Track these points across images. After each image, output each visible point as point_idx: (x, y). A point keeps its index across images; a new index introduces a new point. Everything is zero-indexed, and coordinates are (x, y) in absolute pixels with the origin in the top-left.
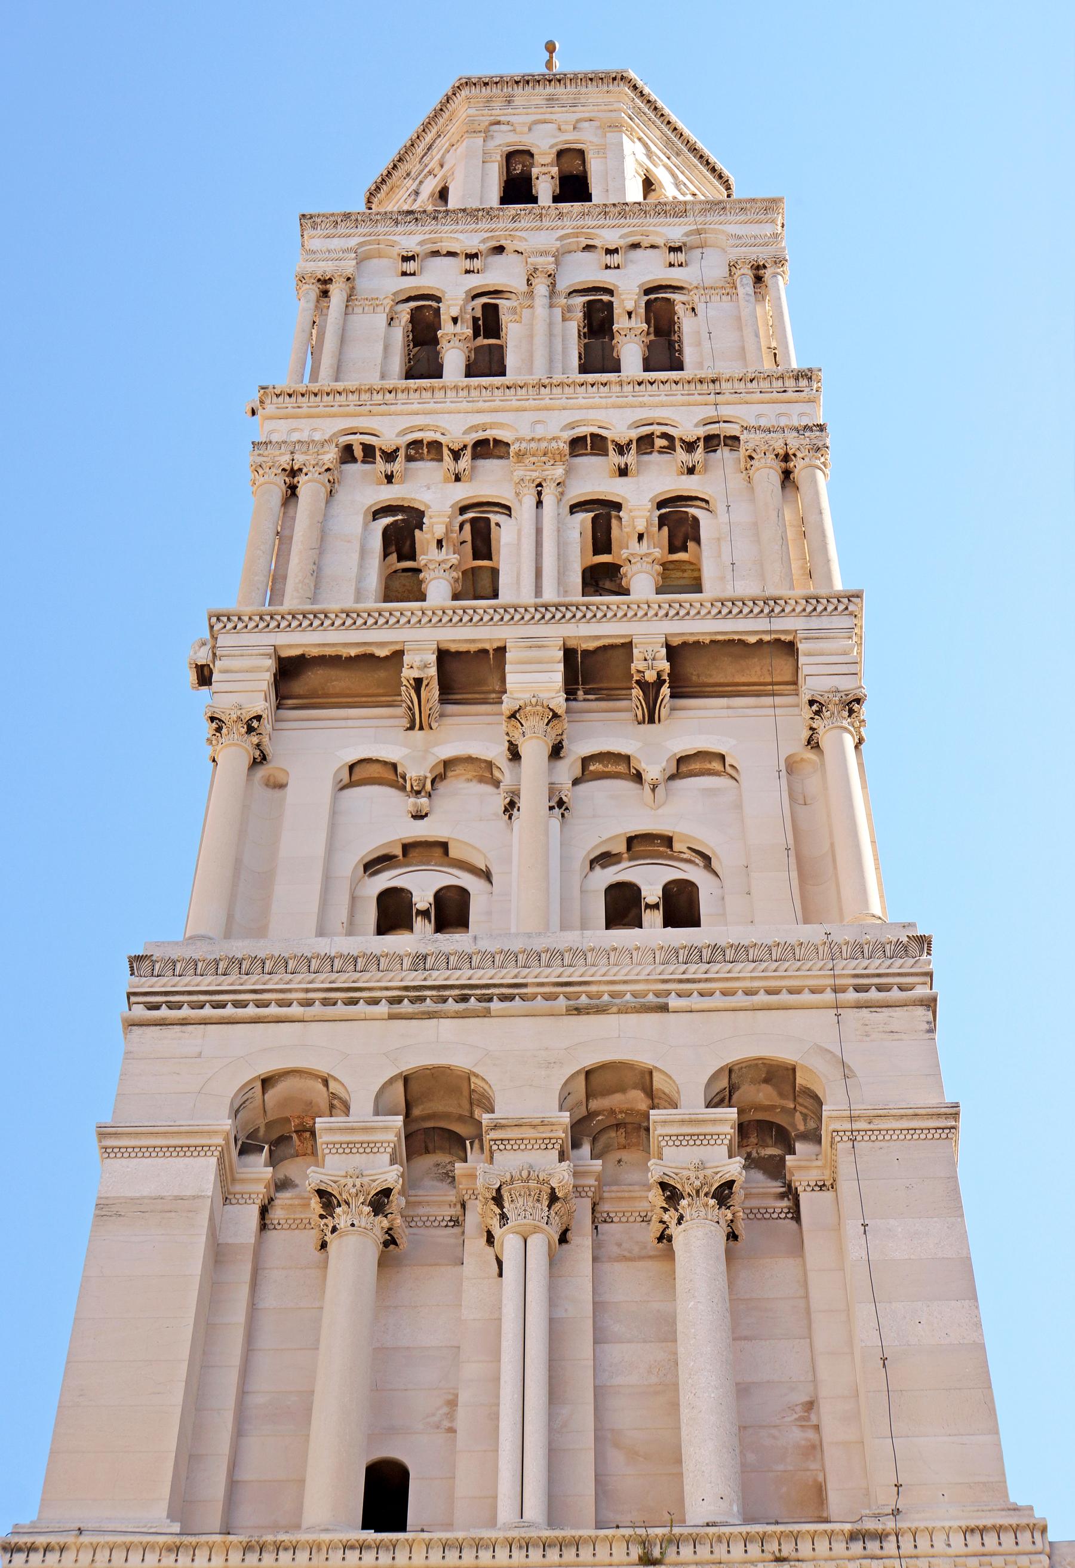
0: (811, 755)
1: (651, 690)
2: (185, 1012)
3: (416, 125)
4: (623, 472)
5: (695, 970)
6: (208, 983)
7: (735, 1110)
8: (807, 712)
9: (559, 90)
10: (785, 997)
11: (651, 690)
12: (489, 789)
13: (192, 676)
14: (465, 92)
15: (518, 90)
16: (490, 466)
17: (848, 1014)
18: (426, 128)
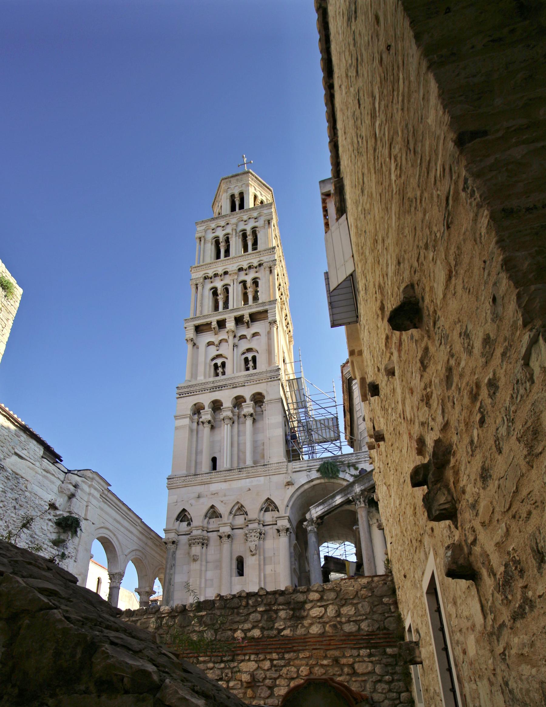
10: (261, 381)
11: (248, 323)
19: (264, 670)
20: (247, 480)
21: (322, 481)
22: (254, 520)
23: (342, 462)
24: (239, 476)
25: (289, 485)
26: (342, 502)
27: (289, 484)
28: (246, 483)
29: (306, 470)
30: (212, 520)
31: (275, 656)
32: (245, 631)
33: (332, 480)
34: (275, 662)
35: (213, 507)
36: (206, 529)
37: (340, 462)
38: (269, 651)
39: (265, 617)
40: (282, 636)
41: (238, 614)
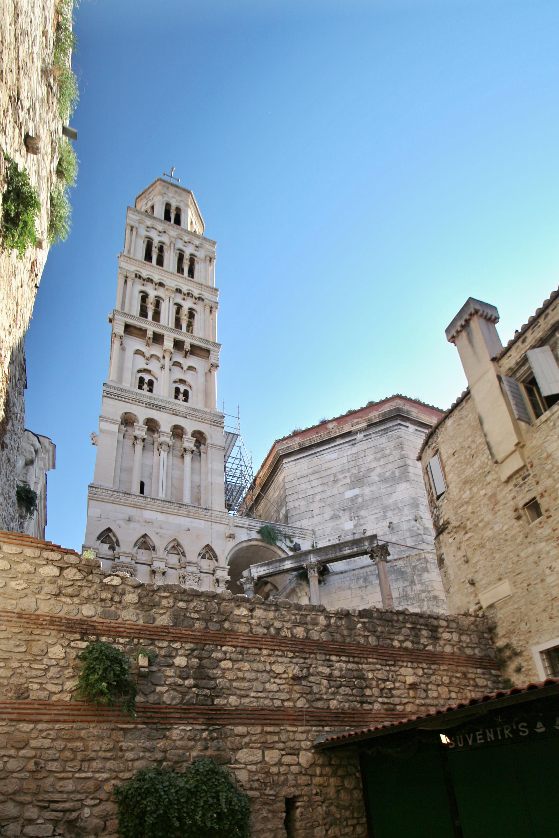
0: (209, 373)
1: (186, 352)
2: (112, 396)
3: (148, 186)
4: (184, 299)
5: (191, 412)
6: (116, 392)
7: (195, 439)
8: (210, 366)
9: (178, 190)
10: (203, 420)
11: (186, 352)
12: (158, 362)
13: (108, 320)
14: (159, 182)
15: (170, 186)
16: (161, 289)
17: (213, 427)
18: (151, 186)
19: (419, 676)
20: (187, 519)
21: (260, 544)
22: (194, 563)
23: (280, 531)
24: (179, 511)
25: (230, 537)
26: (292, 568)
27: (232, 536)
28: (186, 522)
29: (247, 528)
30: (141, 551)
31: (424, 665)
32: (401, 642)
33: (268, 546)
34: (426, 671)
35: (145, 536)
36: (135, 559)
37: (278, 530)
38: (420, 661)
39: (413, 633)
40: (427, 651)
41: (393, 626)
